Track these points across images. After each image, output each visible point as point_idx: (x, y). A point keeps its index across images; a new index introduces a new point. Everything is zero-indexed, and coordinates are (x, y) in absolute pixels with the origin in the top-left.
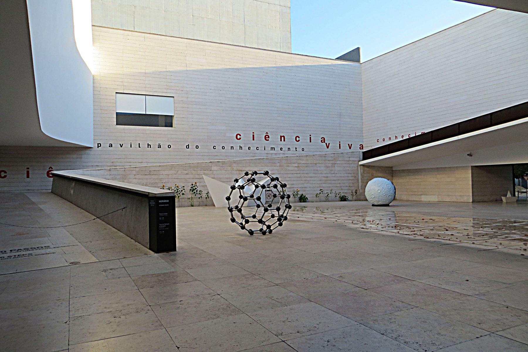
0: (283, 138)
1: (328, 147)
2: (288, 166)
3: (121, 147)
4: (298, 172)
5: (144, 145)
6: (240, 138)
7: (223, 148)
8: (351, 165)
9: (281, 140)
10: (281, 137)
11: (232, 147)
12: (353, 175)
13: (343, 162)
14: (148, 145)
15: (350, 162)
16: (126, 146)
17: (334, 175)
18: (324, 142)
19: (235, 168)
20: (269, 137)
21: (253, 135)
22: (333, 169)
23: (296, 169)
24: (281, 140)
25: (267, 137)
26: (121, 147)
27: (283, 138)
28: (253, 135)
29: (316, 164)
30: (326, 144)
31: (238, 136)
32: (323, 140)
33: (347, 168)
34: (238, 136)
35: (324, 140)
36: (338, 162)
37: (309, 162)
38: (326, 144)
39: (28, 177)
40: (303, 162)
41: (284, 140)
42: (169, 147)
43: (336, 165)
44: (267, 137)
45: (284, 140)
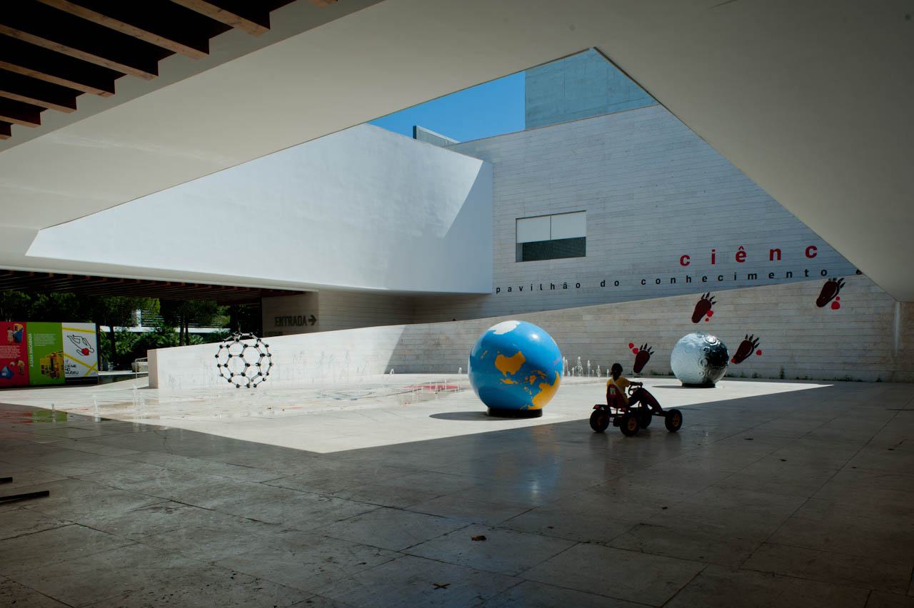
3: (521, 290)
5: (547, 287)
7: (658, 281)
9: (772, 259)
10: (772, 252)
11: (673, 280)
16: (527, 288)
20: (745, 255)
21: (713, 256)
24: (772, 259)
26: (521, 290)
28: (713, 256)
31: (685, 259)
34: (685, 259)
41: (779, 258)
42: (578, 286)
44: (741, 256)
45: (779, 258)
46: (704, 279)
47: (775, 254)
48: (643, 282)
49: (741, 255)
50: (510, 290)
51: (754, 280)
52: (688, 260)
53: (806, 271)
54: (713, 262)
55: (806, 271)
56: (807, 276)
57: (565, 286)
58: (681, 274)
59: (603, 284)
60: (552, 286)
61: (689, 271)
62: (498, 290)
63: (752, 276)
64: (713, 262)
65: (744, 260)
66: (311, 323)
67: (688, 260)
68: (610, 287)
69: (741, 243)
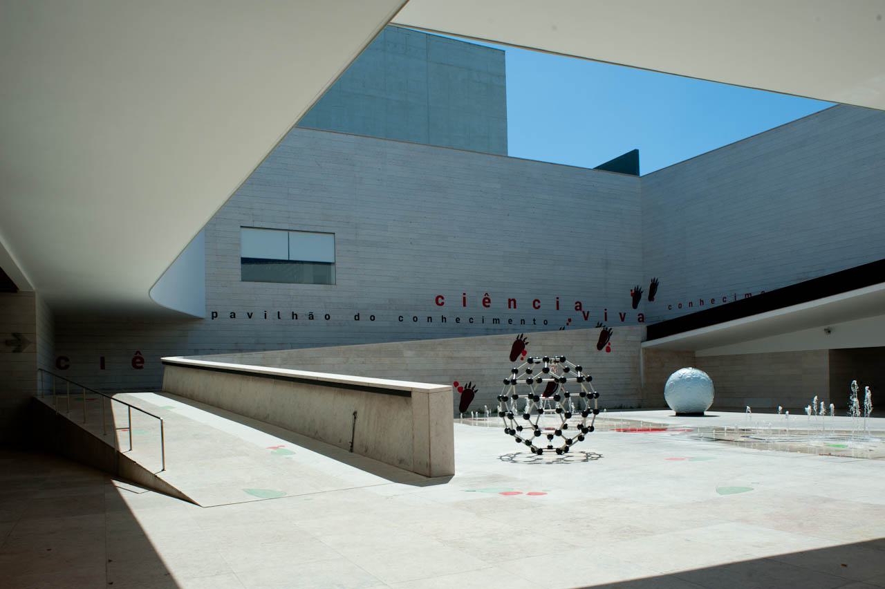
0: (512, 302)
1: (586, 318)
3: (250, 317)
5: (286, 316)
6: (443, 304)
9: (510, 307)
10: (510, 300)
11: (430, 319)
14: (293, 314)
18: (580, 309)
20: (489, 302)
24: (510, 307)
25: (486, 302)
26: (250, 317)
27: (512, 302)
30: (584, 312)
31: (440, 299)
32: (579, 306)
35: (580, 306)
38: (584, 312)
39: (103, 367)
42: (327, 317)
45: (515, 307)
46: (458, 320)
47: (512, 302)
48: (400, 319)
49: (487, 301)
50: (233, 315)
51: (498, 324)
52: (443, 301)
53: (534, 320)
54: (464, 305)
55: (534, 320)
56: (535, 324)
57: (311, 317)
58: (437, 313)
59: (357, 317)
60: (295, 316)
61: (444, 311)
62: (214, 315)
63: (496, 321)
64: (464, 305)
65: (489, 306)
66: (13, 348)
67: (443, 301)
68: (365, 322)
69: (486, 290)
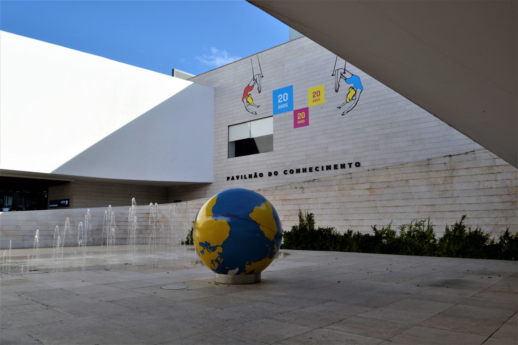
2: (352, 189)
4: (372, 198)
8: (499, 177)
12: (506, 198)
13: (478, 171)
15: (496, 170)
17: (450, 201)
19: (278, 197)
22: (448, 187)
23: (367, 192)
29: (407, 181)
33: (488, 184)
36: (462, 173)
37: (392, 178)
40: (380, 180)
43: (455, 180)
